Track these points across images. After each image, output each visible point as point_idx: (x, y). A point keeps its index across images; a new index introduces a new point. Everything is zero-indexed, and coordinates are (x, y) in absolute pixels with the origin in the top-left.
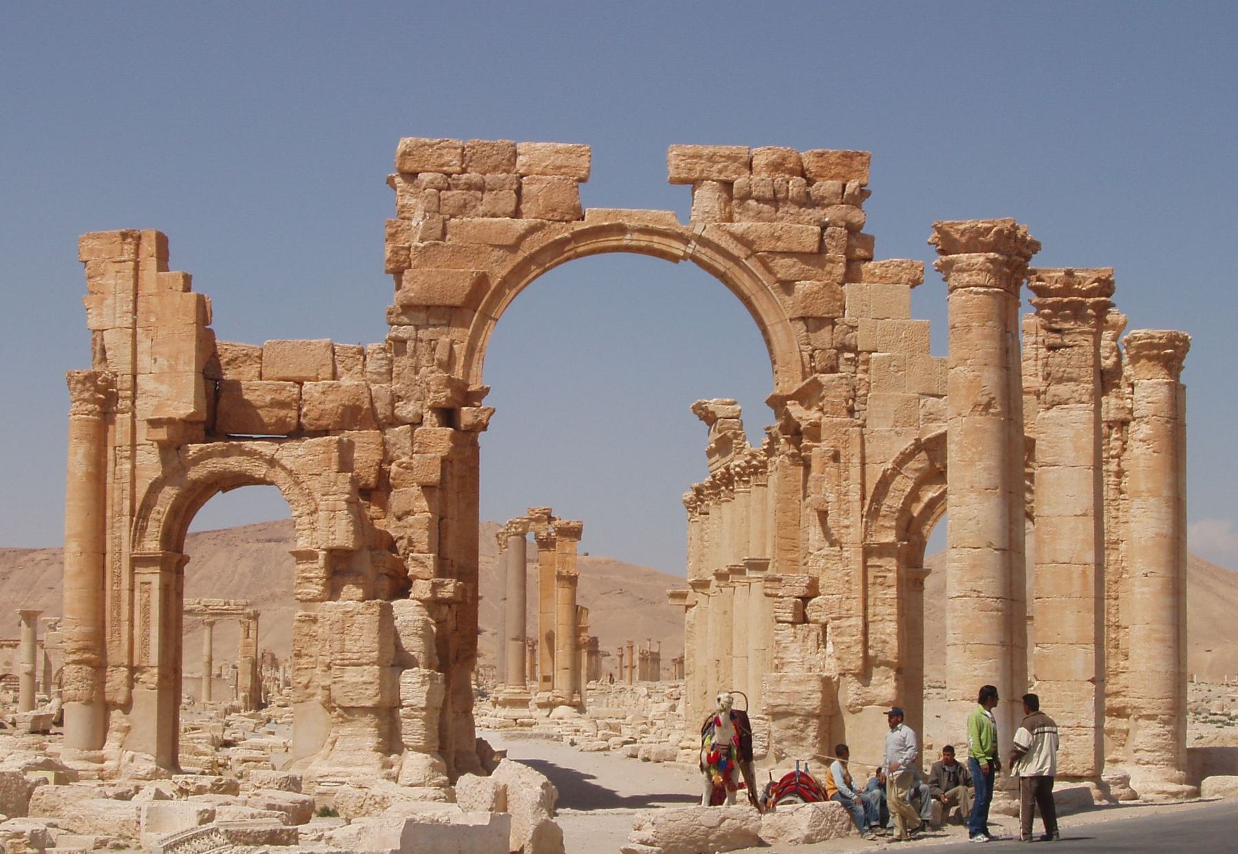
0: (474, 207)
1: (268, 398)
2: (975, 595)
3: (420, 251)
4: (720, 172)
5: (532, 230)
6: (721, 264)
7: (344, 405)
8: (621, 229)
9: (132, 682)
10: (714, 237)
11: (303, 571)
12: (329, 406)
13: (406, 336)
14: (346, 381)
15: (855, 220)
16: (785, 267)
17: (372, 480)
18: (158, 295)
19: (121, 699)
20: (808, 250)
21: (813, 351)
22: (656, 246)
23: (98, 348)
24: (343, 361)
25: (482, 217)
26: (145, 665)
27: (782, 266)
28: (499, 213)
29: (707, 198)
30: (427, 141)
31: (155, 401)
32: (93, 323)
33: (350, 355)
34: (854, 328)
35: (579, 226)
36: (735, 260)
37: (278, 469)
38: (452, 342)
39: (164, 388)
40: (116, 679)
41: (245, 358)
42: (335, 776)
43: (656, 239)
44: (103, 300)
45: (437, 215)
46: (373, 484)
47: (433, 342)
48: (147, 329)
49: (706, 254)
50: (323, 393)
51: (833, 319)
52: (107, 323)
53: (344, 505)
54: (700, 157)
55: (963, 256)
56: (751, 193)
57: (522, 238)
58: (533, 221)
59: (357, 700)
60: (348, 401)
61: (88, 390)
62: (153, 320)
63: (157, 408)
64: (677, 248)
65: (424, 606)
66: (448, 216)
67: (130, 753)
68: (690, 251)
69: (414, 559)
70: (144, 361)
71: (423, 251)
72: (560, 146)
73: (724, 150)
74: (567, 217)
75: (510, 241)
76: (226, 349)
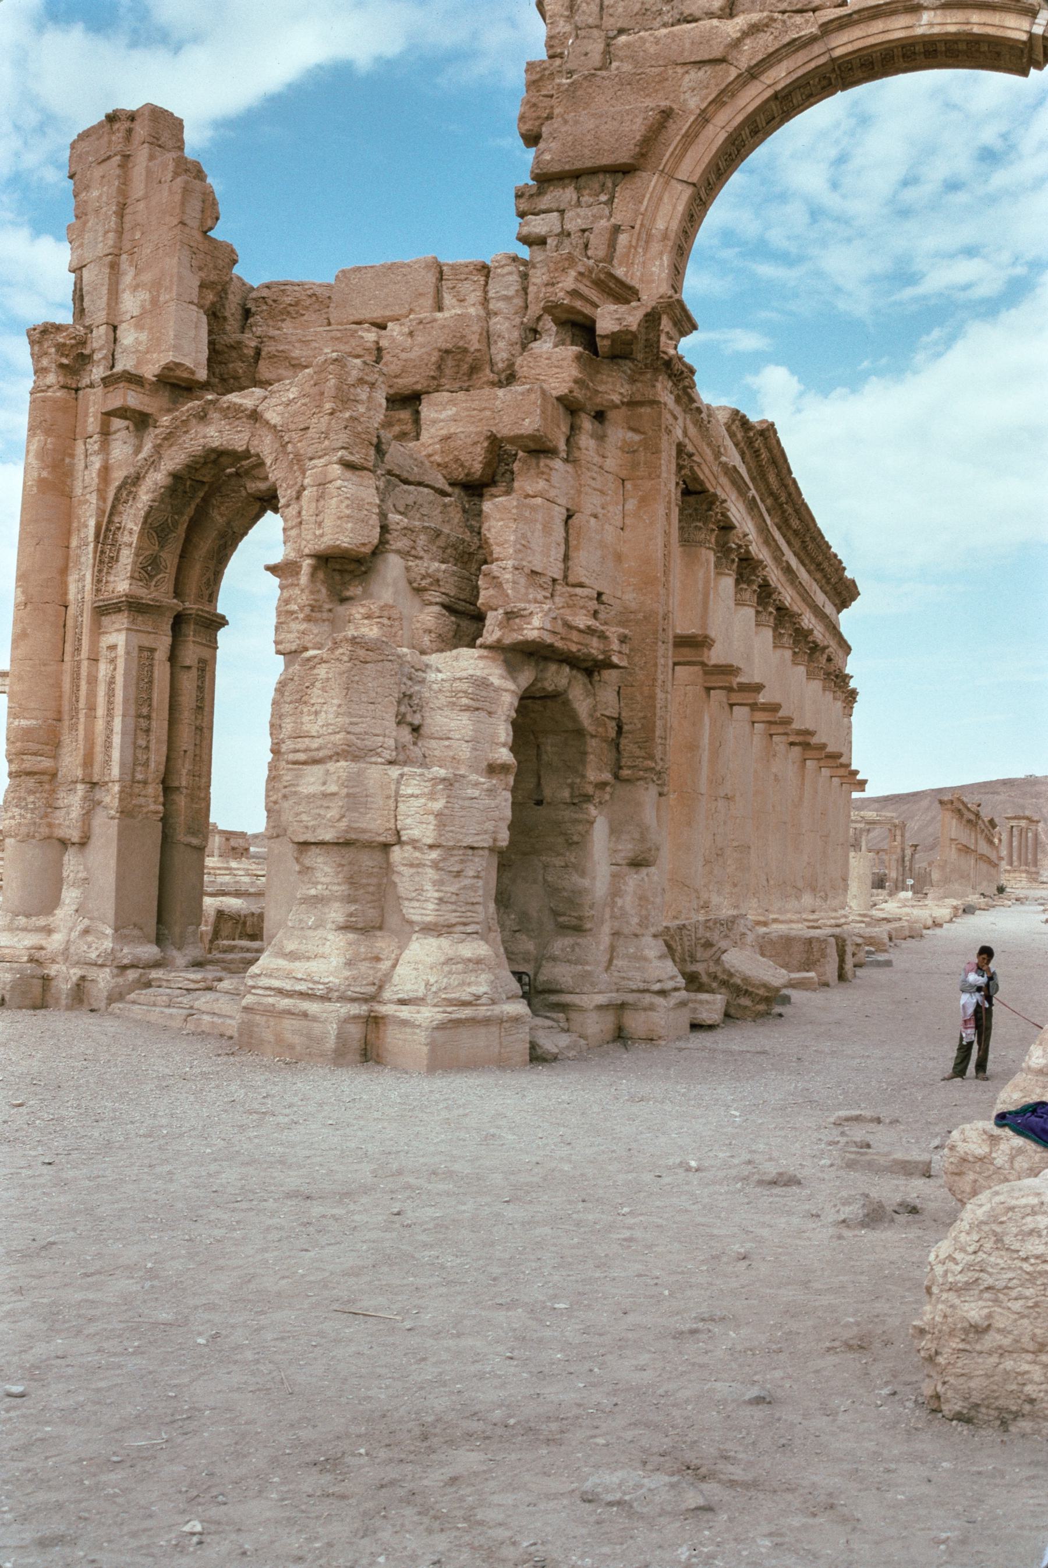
3: (567, 90)
5: (754, 29)
7: (440, 350)
9: (92, 805)
14: (452, 310)
17: (477, 468)
19: (75, 836)
24: (454, 287)
25: (673, 25)
26: (107, 779)
28: (698, 13)
33: (463, 277)
37: (264, 431)
38: (616, 230)
40: (73, 802)
41: (308, 302)
42: (270, 976)
45: (595, 32)
46: (479, 473)
47: (587, 233)
50: (411, 334)
53: (336, 470)
57: (737, 43)
58: (755, 17)
59: (314, 829)
60: (447, 342)
62: (138, 236)
65: (494, 660)
66: (615, 32)
67: (86, 922)
70: (131, 303)
71: (572, 89)
75: (717, 53)
76: (283, 291)
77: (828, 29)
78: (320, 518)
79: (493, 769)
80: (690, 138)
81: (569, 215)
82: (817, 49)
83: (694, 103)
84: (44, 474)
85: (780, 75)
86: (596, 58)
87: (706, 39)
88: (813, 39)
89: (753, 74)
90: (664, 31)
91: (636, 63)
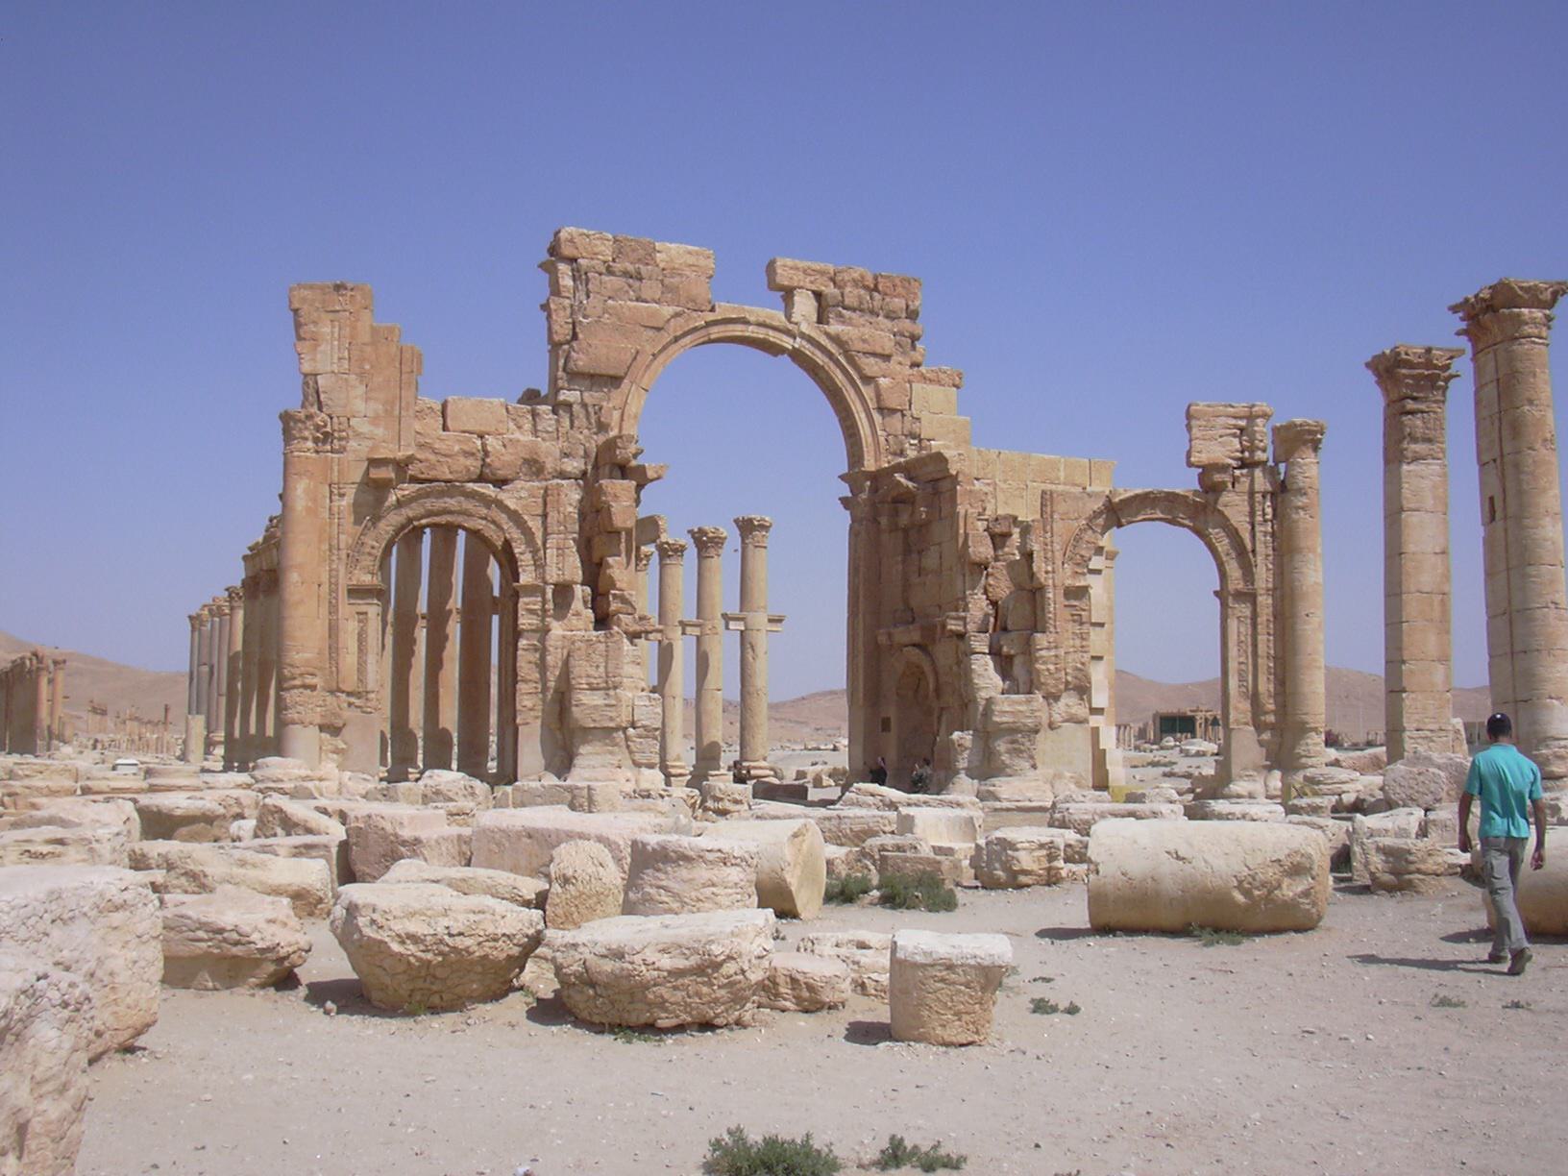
0: (627, 292)
1: (457, 448)
2: (1553, 606)
4: (812, 282)
5: (677, 315)
6: (820, 358)
8: (745, 322)
10: (814, 334)
11: (528, 604)
12: (507, 458)
13: (572, 400)
15: (916, 332)
16: (871, 366)
18: (373, 343)
20: (887, 352)
21: (889, 435)
22: (771, 339)
23: (311, 391)
27: (867, 364)
29: (804, 306)
30: (585, 231)
31: (370, 443)
32: (307, 367)
34: (918, 419)
35: (711, 317)
36: (830, 355)
39: (380, 432)
43: (771, 332)
44: (317, 346)
48: (361, 375)
49: (808, 349)
51: (902, 411)
52: (320, 368)
54: (797, 269)
55: (1525, 311)
56: (843, 302)
57: (669, 320)
58: (679, 309)
61: (306, 428)
62: (367, 367)
63: (372, 449)
64: (788, 343)
68: (797, 346)
69: (614, 595)
72: (690, 248)
73: (817, 266)
74: (704, 308)
77: (709, 324)
78: (560, 565)
81: (586, 394)
82: (703, 332)
83: (649, 349)
84: (310, 504)
86: (599, 311)
87: (653, 314)
88: (702, 328)
90: (629, 303)
91: (619, 319)
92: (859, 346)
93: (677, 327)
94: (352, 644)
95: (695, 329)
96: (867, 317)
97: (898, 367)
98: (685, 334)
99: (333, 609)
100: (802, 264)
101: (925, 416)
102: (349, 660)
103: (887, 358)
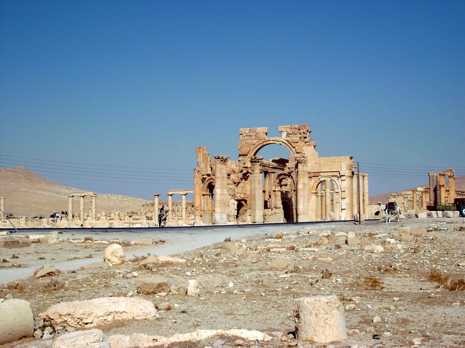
5: (257, 142)
8: (270, 141)
16: (294, 145)
35: (264, 140)
77: (263, 142)
79: (236, 209)
80: (252, 152)
83: (252, 148)
85: (259, 146)
87: (253, 142)
89: (257, 146)
92: (292, 141)
93: (257, 144)
94: (203, 203)
95: (260, 144)
96: (295, 135)
97: (300, 144)
98: (258, 145)
99: (201, 198)
100: (283, 127)
101: (306, 153)
102: (203, 205)
103: (297, 143)
